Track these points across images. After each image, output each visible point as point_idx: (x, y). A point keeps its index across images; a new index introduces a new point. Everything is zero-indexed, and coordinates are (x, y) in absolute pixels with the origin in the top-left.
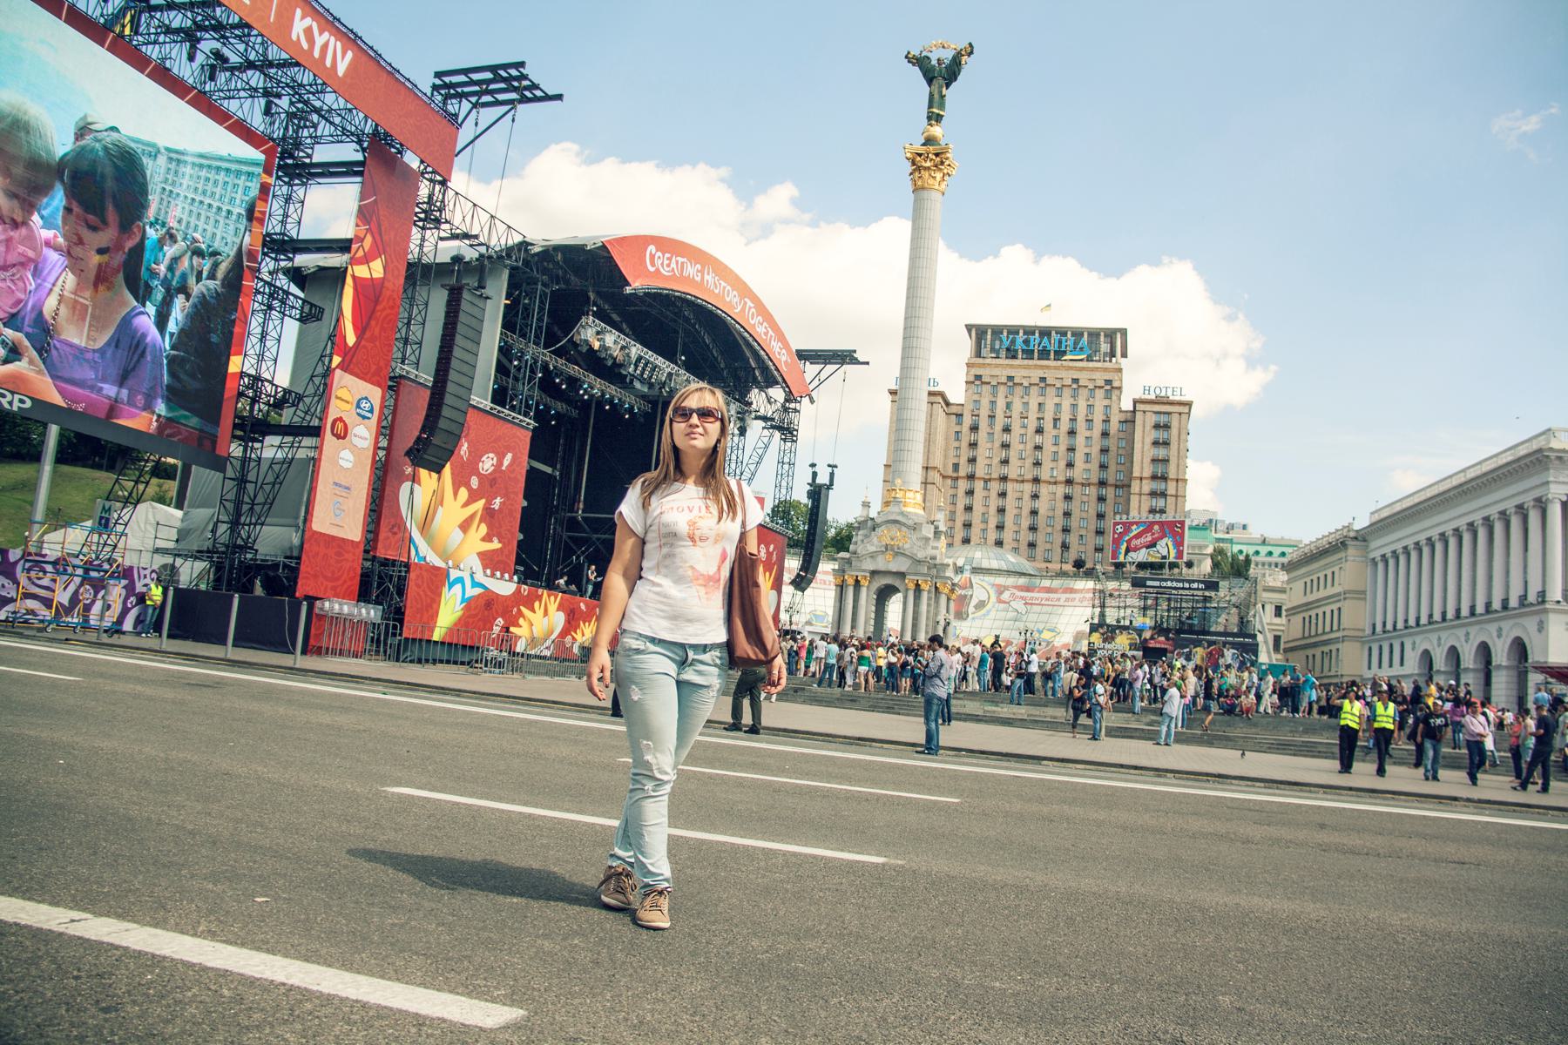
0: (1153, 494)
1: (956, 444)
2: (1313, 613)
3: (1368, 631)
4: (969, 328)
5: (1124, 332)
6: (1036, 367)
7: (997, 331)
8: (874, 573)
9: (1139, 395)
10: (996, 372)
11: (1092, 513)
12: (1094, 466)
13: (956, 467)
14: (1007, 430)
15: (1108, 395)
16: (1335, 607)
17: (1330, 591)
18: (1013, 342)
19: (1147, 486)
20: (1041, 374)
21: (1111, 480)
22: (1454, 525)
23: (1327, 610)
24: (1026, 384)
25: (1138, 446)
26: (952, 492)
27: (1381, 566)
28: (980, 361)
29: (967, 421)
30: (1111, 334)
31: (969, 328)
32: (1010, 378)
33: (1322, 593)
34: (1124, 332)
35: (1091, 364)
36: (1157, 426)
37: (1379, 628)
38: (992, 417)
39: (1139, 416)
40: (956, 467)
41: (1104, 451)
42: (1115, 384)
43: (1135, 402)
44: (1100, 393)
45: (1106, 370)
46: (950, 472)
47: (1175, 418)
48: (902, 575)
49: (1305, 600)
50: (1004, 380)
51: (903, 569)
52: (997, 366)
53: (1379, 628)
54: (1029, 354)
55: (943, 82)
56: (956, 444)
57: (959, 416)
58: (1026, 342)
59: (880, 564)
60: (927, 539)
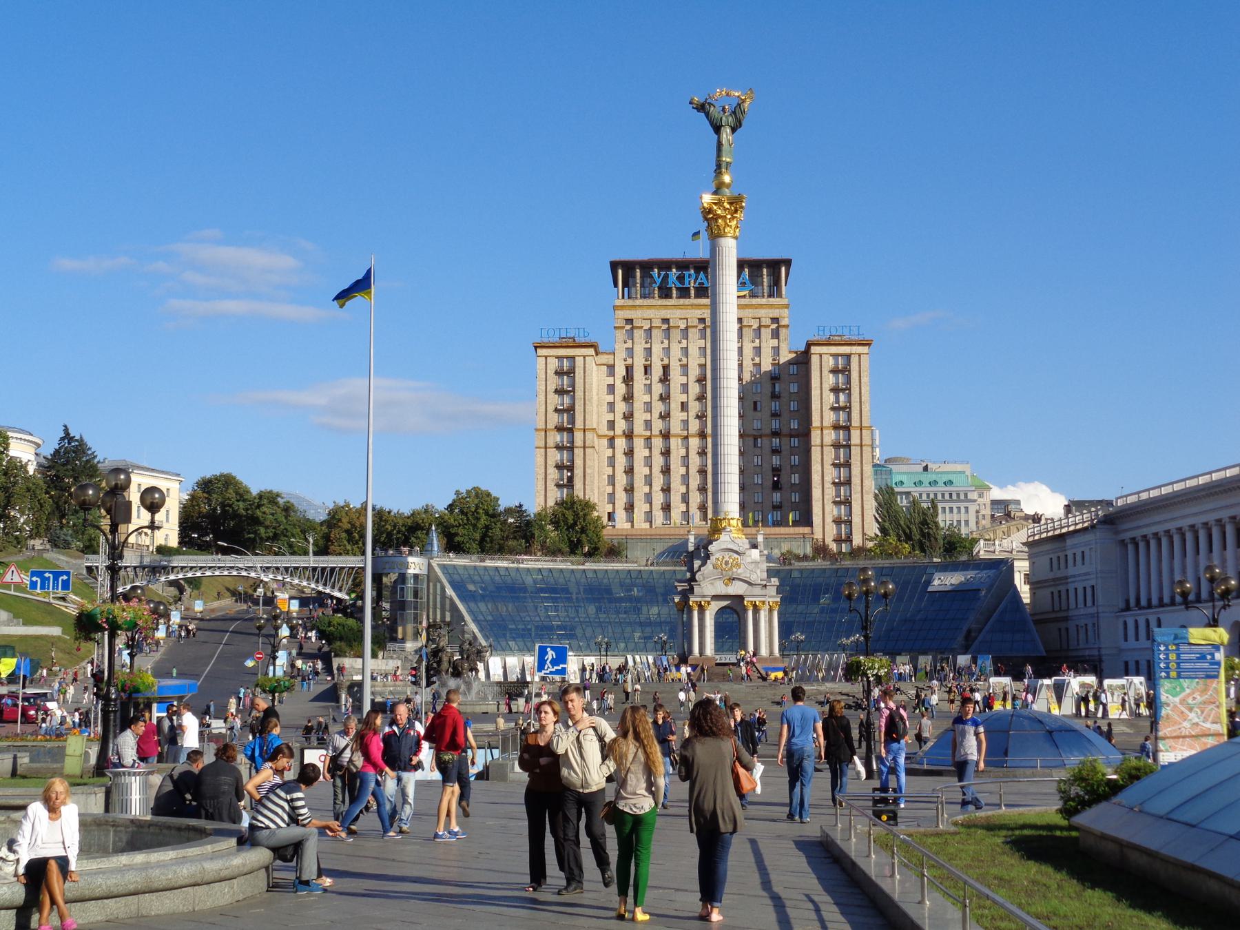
0: (836, 446)
1: (610, 398)
2: (1063, 588)
3: (1122, 605)
4: (614, 266)
5: (788, 263)
6: (693, 306)
7: (647, 266)
8: (716, 598)
9: (812, 338)
10: (650, 313)
11: (767, 468)
12: (766, 414)
13: (611, 425)
14: (665, 379)
15: (776, 334)
16: (1088, 584)
17: (1080, 569)
18: (666, 277)
19: (830, 436)
20: (699, 313)
21: (785, 431)
22: (1204, 519)
23: (1076, 585)
24: (683, 326)
25: (815, 393)
26: (609, 452)
27: (1130, 547)
28: (630, 302)
29: (620, 371)
30: (775, 266)
31: (614, 266)
32: (666, 321)
33: (1071, 571)
34: (788, 263)
35: (755, 301)
36: (835, 371)
37: (1132, 602)
38: (647, 369)
39: (815, 360)
40: (611, 425)
41: (775, 396)
42: (784, 322)
43: (809, 345)
44: (766, 333)
45: (771, 306)
46: (604, 430)
47: (854, 360)
48: (740, 598)
49: (1051, 576)
50: (657, 323)
51: (740, 593)
52: (650, 307)
53: (1132, 602)
54: (684, 293)
55: (728, 130)
56: (610, 398)
57: (611, 368)
58: (681, 279)
59: (721, 589)
60: (756, 563)
